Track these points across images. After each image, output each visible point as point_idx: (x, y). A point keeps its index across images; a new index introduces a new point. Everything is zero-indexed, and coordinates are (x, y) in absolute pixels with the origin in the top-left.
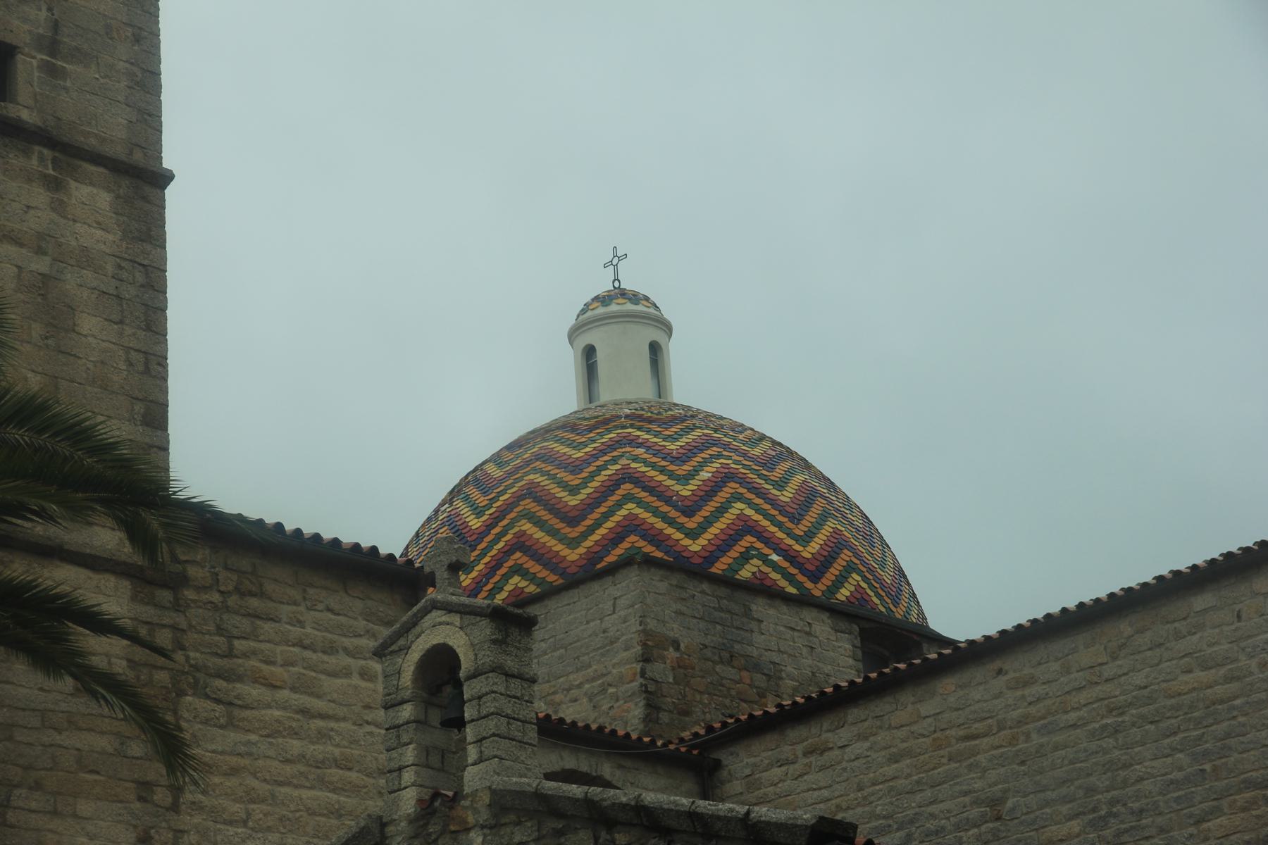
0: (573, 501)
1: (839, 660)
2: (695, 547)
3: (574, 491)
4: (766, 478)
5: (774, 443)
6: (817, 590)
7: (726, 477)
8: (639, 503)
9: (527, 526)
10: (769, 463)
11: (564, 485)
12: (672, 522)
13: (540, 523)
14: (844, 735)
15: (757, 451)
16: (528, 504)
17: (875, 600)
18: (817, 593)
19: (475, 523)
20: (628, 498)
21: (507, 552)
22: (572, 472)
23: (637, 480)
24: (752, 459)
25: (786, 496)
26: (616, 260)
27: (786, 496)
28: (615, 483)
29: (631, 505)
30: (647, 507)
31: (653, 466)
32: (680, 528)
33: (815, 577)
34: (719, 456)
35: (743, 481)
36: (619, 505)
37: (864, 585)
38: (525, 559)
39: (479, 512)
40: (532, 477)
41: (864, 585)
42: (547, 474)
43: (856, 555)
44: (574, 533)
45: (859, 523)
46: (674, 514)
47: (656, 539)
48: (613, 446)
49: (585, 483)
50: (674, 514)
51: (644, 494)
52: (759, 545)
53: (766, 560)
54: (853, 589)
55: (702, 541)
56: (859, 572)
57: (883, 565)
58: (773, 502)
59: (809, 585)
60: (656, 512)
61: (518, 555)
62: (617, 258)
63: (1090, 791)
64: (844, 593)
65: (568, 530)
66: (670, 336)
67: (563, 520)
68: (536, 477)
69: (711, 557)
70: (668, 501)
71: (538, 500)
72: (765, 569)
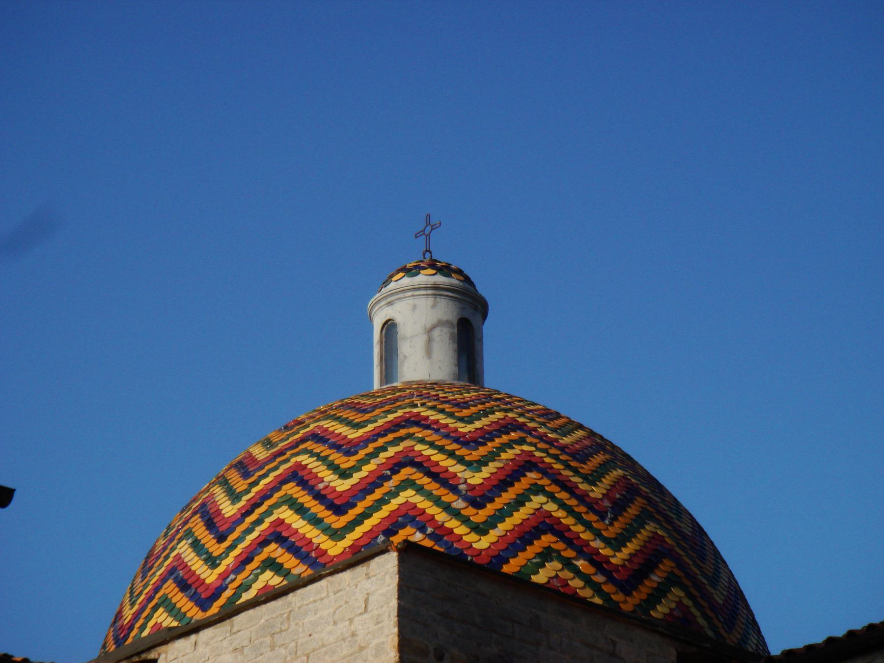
0: (343, 486)
2: (483, 543)
3: (345, 474)
4: (576, 471)
5: (592, 434)
7: (527, 464)
8: (420, 490)
9: (286, 514)
10: (581, 455)
11: (334, 467)
12: (456, 514)
13: (301, 510)
15: (566, 440)
16: (291, 489)
17: (701, 621)
18: (626, 608)
19: (229, 509)
20: (408, 484)
21: (263, 542)
22: (348, 453)
24: (563, 449)
26: (427, 232)
27: (597, 492)
28: (396, 466)
29: (410, 492)
30: (429, 495)
31: (441, 449)
32: (465, 521)
33: (627, 586)
34: (521, 441)
35: (546, 471)
36: (395, 494)
37: (687, 602)
38: (280, 551)
39: (234, 497)
40: (299, 458)
41: (687, 602)
42: (318, 455)
43: (680, 565)
44: (339, 522)
45: (688, 531)
46: (459, 504)
47: (441, 533)
49: (357, 468)
50: (459, 504)
51: (426, 480)
52: (560, 546)
53: (567, 564)
54: (673, 605)
55: (493, 535)
56: (683, 588)
57: (714, 581)
58: (583, 498)
59: (618, 597)
60: (437, 501)
61: (273, 546)
62: (430, 226)
64: (660, 611)
65: (334, 518)
66: (485, 316)
67: (328, 508)
68: (304, 459)
69: (501, 555)
70: (454, 489)
71: (303, 483)
72: (567, 574)
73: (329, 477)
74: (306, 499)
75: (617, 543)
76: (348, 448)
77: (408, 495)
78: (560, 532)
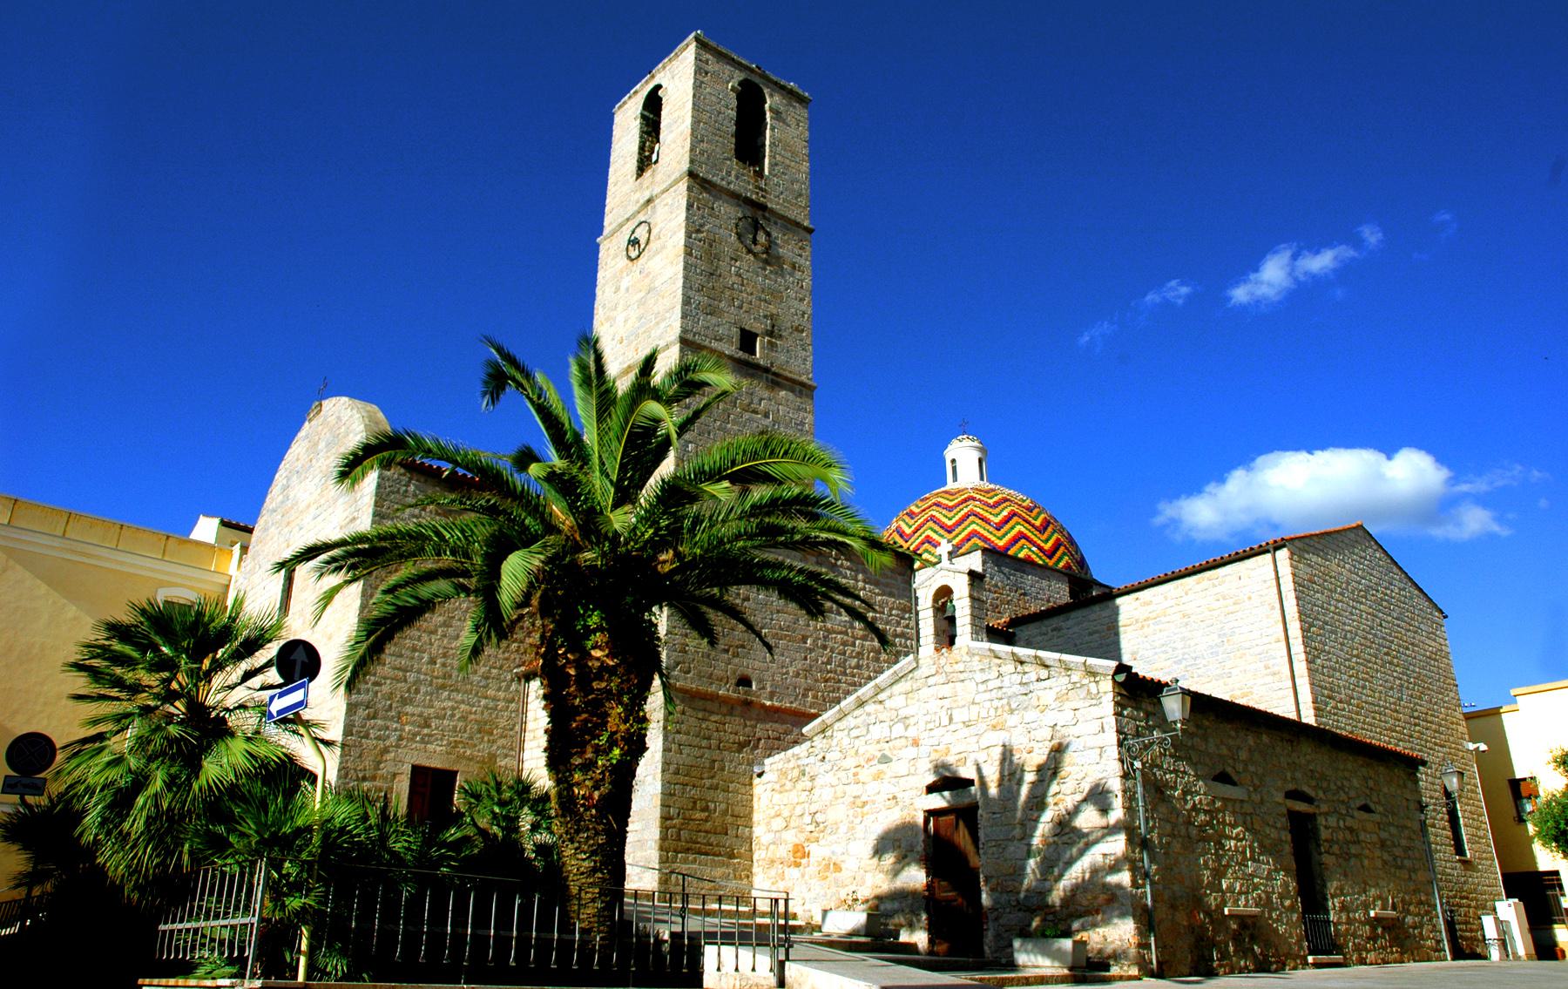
1: (1060, 593)
2: (1001, 543)
6: (1051, 563)
7: (1013, 514)
14: (1070, 623)
16: (931, 524)
19: (908, 531)
23: (976, 515)
25: (1038, 523)
27: (1038, 523)
28: (967, 516)
33: (1050, 557)
47: (986, 540)
48: (965, 501)
63: (1174, 649)
64: (1061, 564)
73: (944, 520)
74: (937, 528)
75: (1047, 541)
76: (950, 509)
77: (973, 527)
78: (1027, 538)
